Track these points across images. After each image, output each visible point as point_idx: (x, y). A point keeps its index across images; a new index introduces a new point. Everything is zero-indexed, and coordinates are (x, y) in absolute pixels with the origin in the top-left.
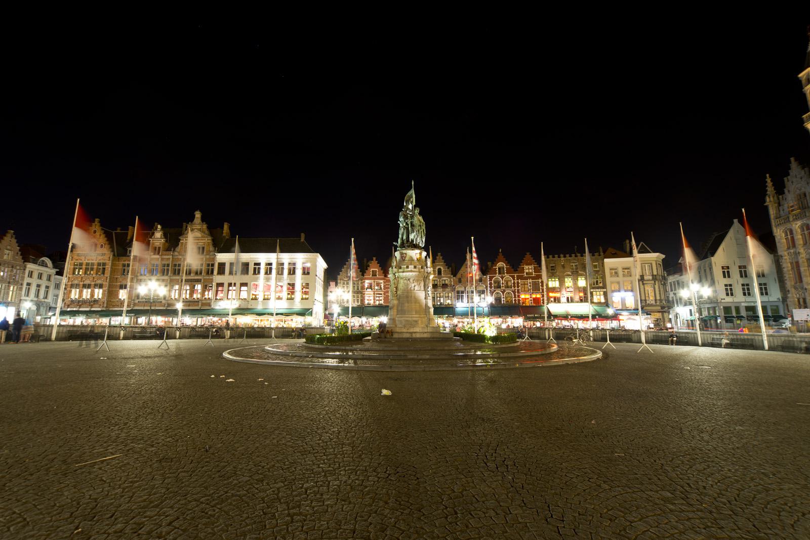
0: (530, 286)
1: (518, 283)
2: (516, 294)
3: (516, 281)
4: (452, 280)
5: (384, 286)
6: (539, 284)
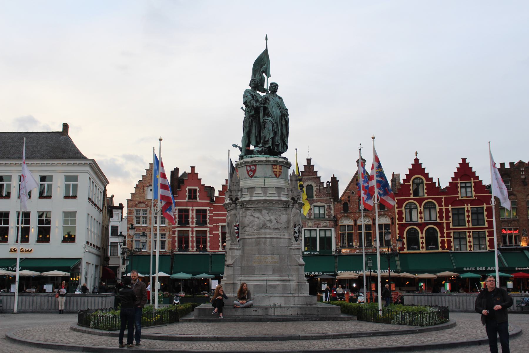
0: (468, 216)
1: (447, 211)
2: (445, 231)
3: (444, 208)
4: (332, 206)
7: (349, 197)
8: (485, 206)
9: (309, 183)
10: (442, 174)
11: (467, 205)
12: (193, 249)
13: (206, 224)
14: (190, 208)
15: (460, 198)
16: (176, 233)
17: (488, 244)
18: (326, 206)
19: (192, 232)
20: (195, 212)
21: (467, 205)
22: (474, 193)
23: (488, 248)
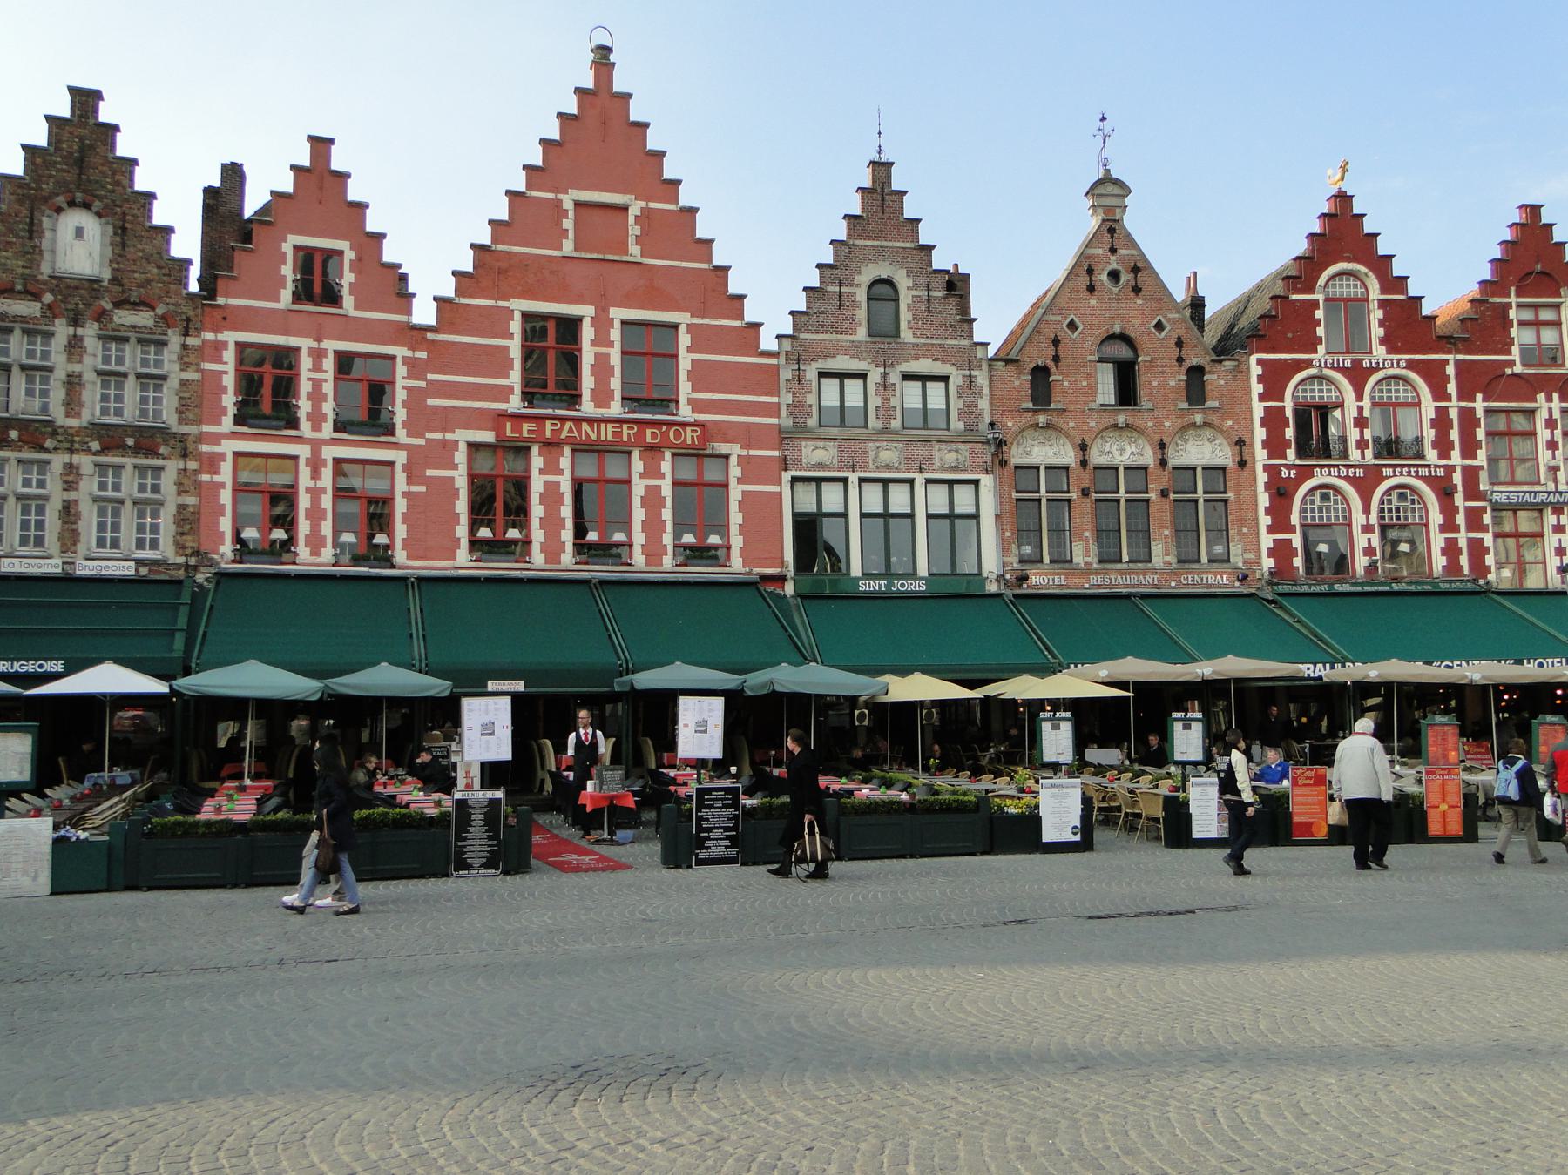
1: (1468, 418)
2: (1459, 499)
3: (1454, 409)
4: (982, 377)
5: (415, 399)
7: (1056, 342)
9: (884, 271)
11: (1549, 399)
12: (316, 552)
13: (390, 431)
14: (304, 343)
15: (1518, 369)
16: (226, 468)
19: (316, 465)
20: (329, 363)
21: (1549, 399)
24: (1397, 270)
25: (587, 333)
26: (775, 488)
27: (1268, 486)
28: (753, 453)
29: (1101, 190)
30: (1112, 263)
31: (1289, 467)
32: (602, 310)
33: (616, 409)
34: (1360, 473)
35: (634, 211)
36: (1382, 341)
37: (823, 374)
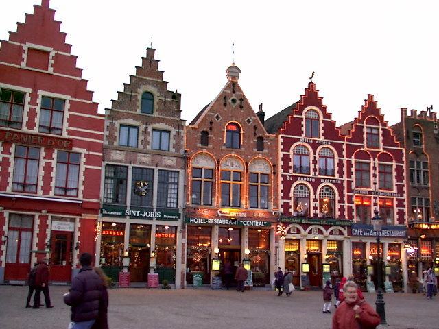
1: (349, 162)
3: (345, 159)
6: (391, 173)
7: (211, 123)
8: (394, 164)
10: (344, 112)
15: (365, 149)
17: (396, 217)
18: (173, 132)
22: (381, 145)
23: (396, 223)
24: (329, 111)
25: (28, 99)
26: (100, 168)
27: (283, 183)
28: (91, 153)
29: (230, 70)
30: (232, 96)
31: (290, 176)
32: (35, 91)
33: (36, 131)
34: (314, 180)
35: (53, 53)
36: (323, 135)
37: (122, 125)
